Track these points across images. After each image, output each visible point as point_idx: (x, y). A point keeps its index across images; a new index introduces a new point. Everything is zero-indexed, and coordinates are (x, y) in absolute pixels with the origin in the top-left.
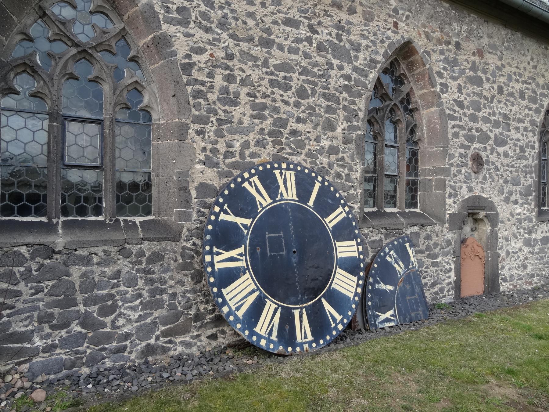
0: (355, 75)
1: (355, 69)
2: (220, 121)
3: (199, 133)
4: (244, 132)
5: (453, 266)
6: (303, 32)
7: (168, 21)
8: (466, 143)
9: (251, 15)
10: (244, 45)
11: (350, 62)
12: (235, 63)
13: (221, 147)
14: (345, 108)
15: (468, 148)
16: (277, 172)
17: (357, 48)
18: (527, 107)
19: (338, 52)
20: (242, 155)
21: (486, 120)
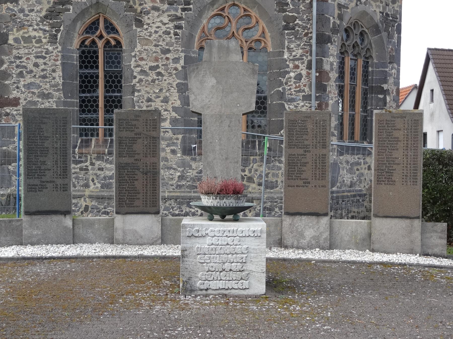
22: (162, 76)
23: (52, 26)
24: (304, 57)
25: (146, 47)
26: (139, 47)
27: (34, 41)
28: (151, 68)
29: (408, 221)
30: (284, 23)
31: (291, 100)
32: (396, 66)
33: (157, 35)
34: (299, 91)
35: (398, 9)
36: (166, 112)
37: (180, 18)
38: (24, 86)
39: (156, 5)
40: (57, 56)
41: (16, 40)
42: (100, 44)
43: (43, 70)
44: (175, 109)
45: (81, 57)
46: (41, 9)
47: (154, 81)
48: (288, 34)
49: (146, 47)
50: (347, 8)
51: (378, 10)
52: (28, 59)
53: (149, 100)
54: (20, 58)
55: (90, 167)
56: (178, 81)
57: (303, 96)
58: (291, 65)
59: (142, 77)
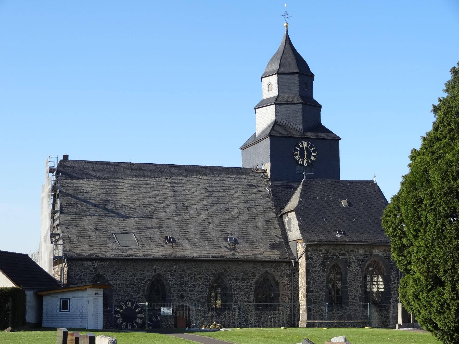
0: (145, 283)
1: (145, 282)
2: (118, 295)
4: (122, 296)
5: (173, 321)
7: (110, 281)
9: (123, 277)
10: (122, 282)
11: (143, 280)
12: (120, 285)
13: (118, 299)
14: (142, 289)
15: (179, 294)
16: (127, 302)
17: (145, 278)
18: (203, 281)
19: (140, 279)
20: (121, 300)
21: (185, 286)
22: (356, 283)
23: (323, 267)
26: (349, 274)
28: (353, 281)
30: (390, 266)
31: (393, 290)
38: (315, 286)
41: (312, 271)
43: (320, 281)
44: (360, 294)
47: (354, 285)
48: (391, 270)
52: (316, 277)
53: (352, 291)
54: (314, 277)
58: (393, 280)
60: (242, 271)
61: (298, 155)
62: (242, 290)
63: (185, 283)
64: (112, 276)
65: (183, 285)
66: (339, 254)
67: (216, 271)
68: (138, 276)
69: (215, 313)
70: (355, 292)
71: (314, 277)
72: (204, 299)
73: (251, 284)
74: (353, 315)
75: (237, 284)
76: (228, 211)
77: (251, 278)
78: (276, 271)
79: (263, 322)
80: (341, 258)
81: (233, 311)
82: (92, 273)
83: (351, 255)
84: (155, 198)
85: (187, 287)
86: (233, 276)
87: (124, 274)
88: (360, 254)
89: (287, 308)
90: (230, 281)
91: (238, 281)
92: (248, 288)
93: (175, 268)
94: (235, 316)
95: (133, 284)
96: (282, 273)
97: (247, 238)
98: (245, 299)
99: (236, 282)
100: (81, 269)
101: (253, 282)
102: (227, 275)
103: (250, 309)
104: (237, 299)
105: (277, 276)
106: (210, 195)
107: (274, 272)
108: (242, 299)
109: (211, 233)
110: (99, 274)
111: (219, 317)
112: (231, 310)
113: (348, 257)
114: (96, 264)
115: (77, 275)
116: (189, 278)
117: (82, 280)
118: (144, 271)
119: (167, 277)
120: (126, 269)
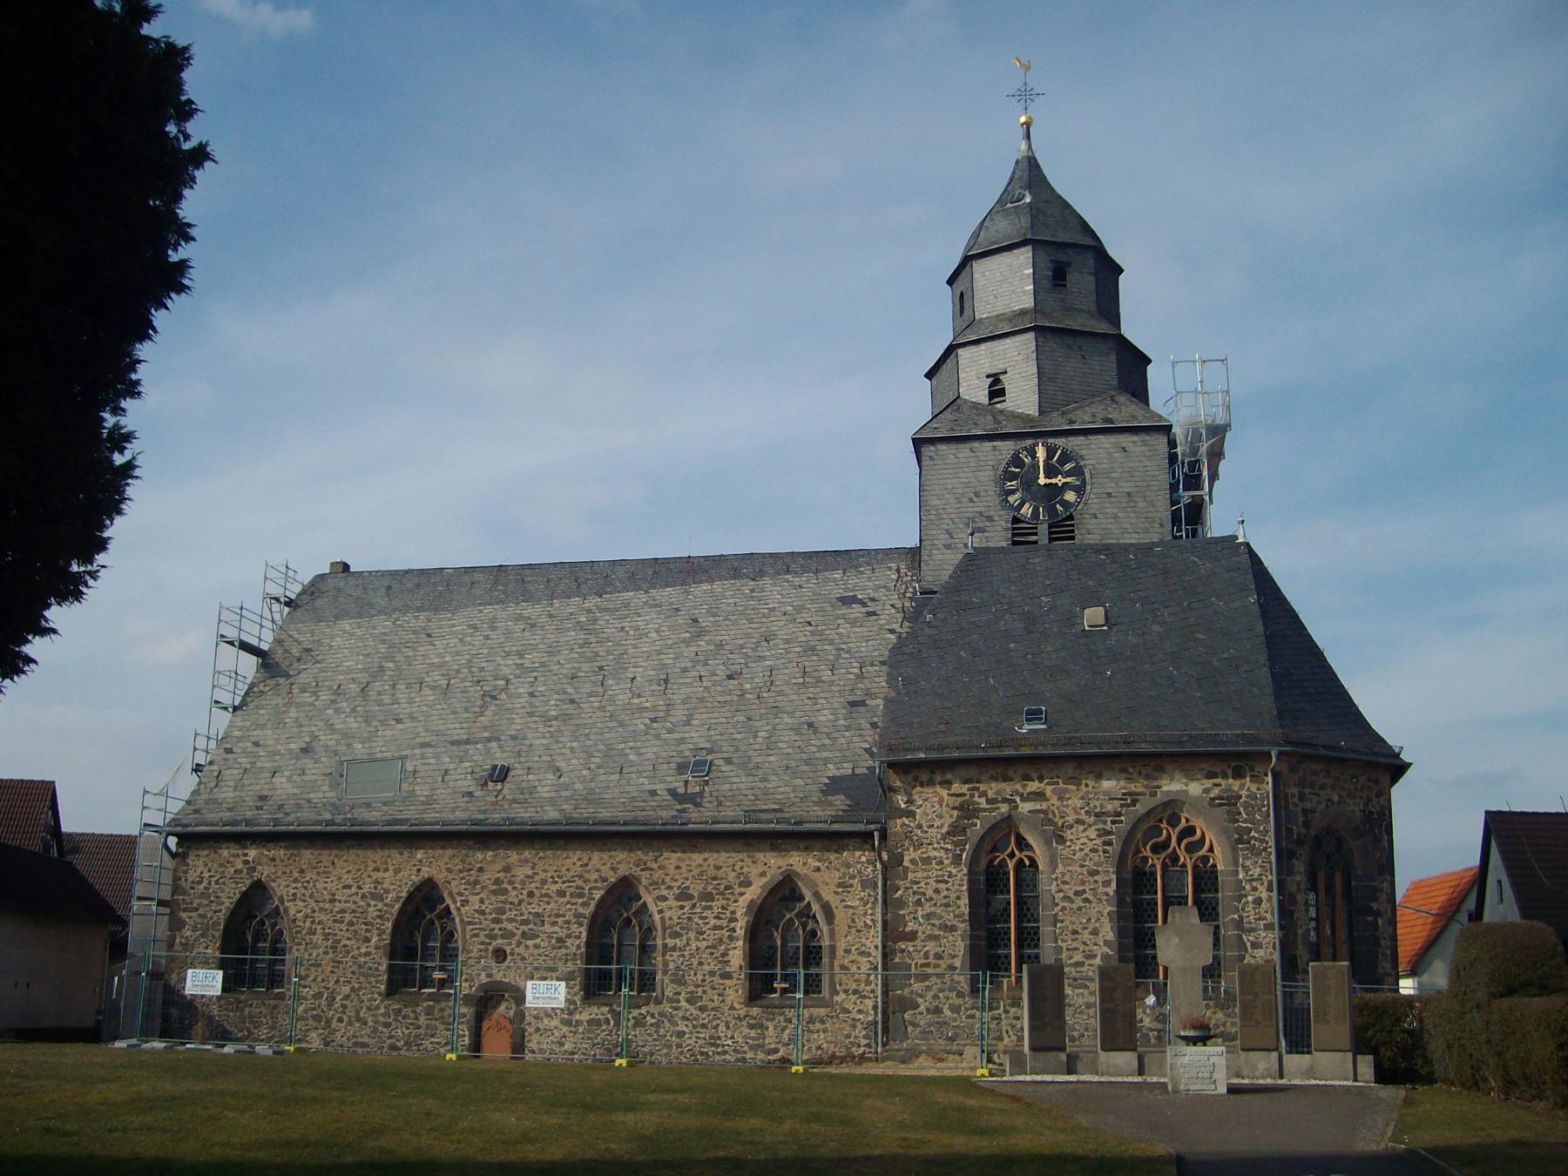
0: (386, 908)
1: (386, 905)
2: (307, 944)
3: (297, 950)
5: (467, 1033)
6: (354, 890)
7: (288, 901)
8: (487, 941)
9: (325, 889)
10: (321, 905)
11: (382, 900)
12: (317, 914)
14: (377, 929)
17: (387, 891)
19: (374, 896)
21: (511, 920)
22: (1090, 902)
23: (956, 844)
24: (1264, 877)
25: (1070, 868)
26: (1060, 868)
27: (934, 862)
28: (1077, 893)
29: (1341, 1054)
30: (1236, 836)
31: (1251, 930)
32: (1388, 878)
33: (1083, 854)
34: (1260, 919)
35: (1386, 803)
36: (1096, 947)
37: (1110, 833)
39: (1080, 817)
40: (962, 880)
41: (913, 861)
42: (1011, 865)
43: (945, 897)
44: (1106, 943)
45: (988, 880)
46: (943, 824)
47: (1080, 909)
49: (1070, 868)
50: (1315, 812)
51: (1357, 809)
54: (918, 883)
55: (1003, 1016)
56: (1110, 909)
57: (1265, 925)
59: (1066, 904)
60: (705, 868)
61: (1017, 490)
62: (702, 933)
63: (510, 910)
64: (294, 885)
65: (504, 917)
66: (1017, 793)
67: (613, 869)
68: (367, 888)
69: (605, 1009)
70: (1086, 936)
71: (918, 883)
72: (569, 964)
73: (733, 913)
74: (1077, 1026)
75: (684, 914)
76: (735, 682)
77: (733, 894)
78: (823, 868)
79: (773, 1046)
80: (1029, 812)
81: (667, 1008)
82: (241, 878)
83: (1067, 796)
84: (521, 656)
85: (517, 921)
86: (670, 888)
87: (329, 880)
88: (1106, 793)
89: (865, 997)
90: (659, 903)
91: (687, 904)
92: (721, 928)
93: (481, 862)
94: (675, 1024)
95: (353, 911)
96: (844, 874)
97: (759, 760)
98: (709, 964)
99: (682, 907)
100: (210, 864)
101: (741, 907)
102: (650, 885)
103: (729, 1000)
104: (682, 963)
105: (827, 884)
106: (699, 635)
107: (818, 869)
108: (701, 964)
109: (643, 750)
110: (259, 880)
111: (617, 1024)
112: (658, 1002)
113: (1058, 803)
114: (252, 853)
115: (200, 882)
116: (525, 892)
117: (212, 898)
118: (386, 870)
119: (455, 891)
120: (333, 863)
